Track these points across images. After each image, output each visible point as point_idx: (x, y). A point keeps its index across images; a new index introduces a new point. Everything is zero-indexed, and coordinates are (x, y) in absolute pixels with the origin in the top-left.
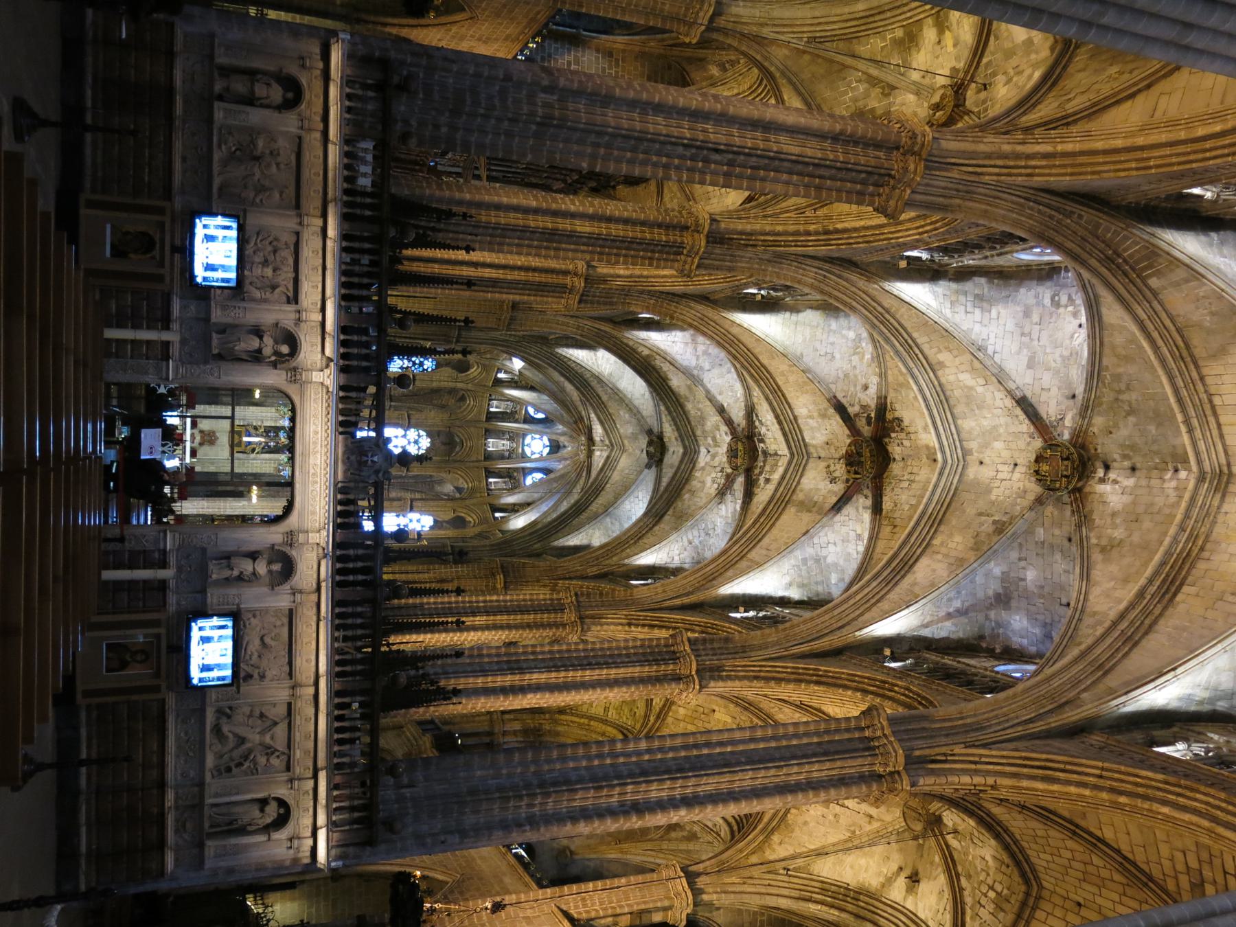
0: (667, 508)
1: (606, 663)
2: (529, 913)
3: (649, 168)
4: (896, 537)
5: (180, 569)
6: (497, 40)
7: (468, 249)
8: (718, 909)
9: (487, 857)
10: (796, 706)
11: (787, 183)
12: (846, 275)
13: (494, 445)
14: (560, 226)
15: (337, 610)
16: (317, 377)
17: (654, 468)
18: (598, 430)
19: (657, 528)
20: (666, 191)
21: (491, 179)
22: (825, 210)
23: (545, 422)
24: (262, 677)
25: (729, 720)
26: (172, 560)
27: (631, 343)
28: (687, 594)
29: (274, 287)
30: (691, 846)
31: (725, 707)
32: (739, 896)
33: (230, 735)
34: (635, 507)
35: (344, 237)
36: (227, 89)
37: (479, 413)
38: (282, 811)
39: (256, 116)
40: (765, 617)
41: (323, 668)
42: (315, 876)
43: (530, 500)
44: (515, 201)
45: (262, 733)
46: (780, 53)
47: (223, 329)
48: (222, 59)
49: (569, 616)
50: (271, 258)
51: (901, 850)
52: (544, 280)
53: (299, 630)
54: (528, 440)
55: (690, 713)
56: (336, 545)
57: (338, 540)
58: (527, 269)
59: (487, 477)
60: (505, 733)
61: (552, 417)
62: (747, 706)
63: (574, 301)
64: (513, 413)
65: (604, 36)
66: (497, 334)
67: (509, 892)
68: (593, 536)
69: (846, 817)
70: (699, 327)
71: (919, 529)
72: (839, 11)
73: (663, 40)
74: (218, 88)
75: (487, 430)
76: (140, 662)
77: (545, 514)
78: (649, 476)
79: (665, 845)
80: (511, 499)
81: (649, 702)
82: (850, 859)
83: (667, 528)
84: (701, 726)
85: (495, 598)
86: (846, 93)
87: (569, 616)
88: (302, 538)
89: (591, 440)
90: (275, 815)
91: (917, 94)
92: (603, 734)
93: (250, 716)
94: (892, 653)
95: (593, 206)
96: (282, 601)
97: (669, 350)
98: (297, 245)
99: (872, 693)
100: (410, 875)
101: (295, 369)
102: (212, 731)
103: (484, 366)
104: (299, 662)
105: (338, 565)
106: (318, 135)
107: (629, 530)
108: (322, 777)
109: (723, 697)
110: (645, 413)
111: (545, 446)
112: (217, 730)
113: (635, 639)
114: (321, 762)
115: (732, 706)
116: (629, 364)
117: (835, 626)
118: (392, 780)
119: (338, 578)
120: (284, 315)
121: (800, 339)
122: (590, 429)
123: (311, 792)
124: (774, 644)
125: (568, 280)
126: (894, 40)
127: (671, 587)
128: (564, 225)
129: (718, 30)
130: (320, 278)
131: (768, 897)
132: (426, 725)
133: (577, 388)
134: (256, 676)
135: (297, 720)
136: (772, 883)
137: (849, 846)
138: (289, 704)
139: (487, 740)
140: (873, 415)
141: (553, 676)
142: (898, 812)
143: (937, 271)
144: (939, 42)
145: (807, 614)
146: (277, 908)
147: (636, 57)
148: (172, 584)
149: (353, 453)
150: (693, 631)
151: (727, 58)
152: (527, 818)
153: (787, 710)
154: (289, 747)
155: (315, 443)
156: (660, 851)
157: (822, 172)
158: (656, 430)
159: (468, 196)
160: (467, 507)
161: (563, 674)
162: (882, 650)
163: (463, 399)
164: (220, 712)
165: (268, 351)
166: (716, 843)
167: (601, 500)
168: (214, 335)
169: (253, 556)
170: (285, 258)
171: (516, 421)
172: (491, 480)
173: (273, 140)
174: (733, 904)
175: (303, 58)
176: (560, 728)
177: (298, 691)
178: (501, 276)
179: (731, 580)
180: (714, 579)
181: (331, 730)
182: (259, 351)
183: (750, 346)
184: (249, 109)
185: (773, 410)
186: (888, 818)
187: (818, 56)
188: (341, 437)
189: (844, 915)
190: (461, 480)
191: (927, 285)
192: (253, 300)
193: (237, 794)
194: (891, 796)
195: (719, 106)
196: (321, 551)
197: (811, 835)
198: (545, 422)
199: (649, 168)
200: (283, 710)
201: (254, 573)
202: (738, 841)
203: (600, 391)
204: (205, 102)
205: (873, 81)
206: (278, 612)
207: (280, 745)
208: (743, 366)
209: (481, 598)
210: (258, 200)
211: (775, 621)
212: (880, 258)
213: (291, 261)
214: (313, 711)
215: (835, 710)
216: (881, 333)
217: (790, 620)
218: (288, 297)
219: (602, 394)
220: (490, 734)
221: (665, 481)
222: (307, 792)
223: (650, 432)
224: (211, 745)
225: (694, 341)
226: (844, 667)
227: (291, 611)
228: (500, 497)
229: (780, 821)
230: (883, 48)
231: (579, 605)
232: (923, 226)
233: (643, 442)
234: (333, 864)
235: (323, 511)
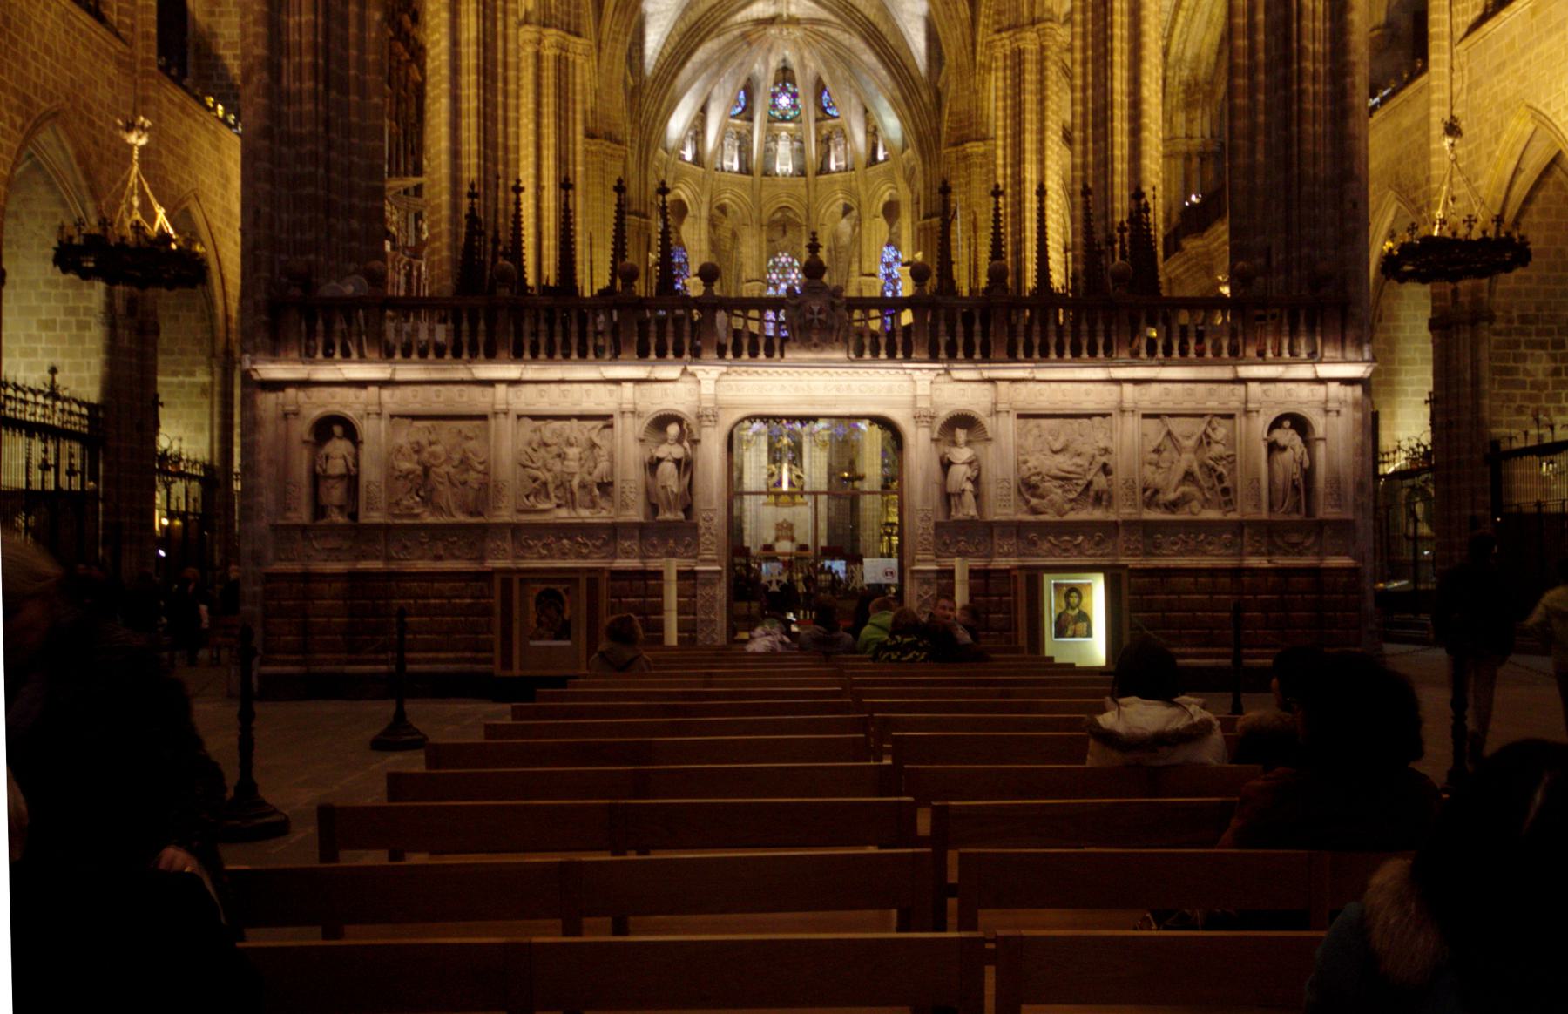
5: (961, 554)
6: (221, 163)
7: (518, 190)
9: (1381, 140)
13: (784, 164)
14: (473, 62)
15: (1021, 356)
16: (708, 388)
21: (418, 171)
23: (749, 89)
24: (1106, 451)
26: (947, 563)
29: (593, 445)
33: (1181, 489)
35: (517, 356)
36: (341, 508)
37: (740, 185)
38: (1287, 424)
39: (371, 472)
41: (1099, 373)
43: (860, 110)
44: (444, 130)
47: (653, 508)
48: (303, 515)
49: (1029, 41)
50: (555, 450)
52: (552, 90)
53: (1045, 405)
56: (934, 358)
57: (926, 357)
58: (538, 114)
59: (829, 172)
60: (1189, 137)
63: (579, 45)
64: (740, 137)
74: (339, 519)
75: (765, 174)
76: (1080, 597)
77: (881, 87)
80: (859, 137)
85: (1000, 152)
87: (1029, 41)
88: (923, 404)
90: (1292, 432)
93: (1157, 466)
95: (438, 11)
96: (1006, 428)
98: (535, 417)
101: (699, 416)
104: (1089, 405)
105: (960, 355)
106: (386, 394)
108: (1245, 371)
112: (1173, 506)
114: (1226, 373)
118: (1260, 279)
119: (977, 356)
120: (628, 433)
123: (1266, 386)
125: (549, 53)
128: (470, 57)
130: (576, 386)
133: (701, 41)
134: (1104, 459)
135: (1167, 405)
138: (1145, 416)
139: (1196, 162)
141: (1120, 58)
148: (978, 563)
149: (809, 339)
154: (1202, 416)
155: (796, 389)
159: (445, 198)
160: (870, 199)
161: (1117, 44)
163: (723, 209)
164: (1150, 503)
165: (678, 452)
168: (660, 517)
169: (946, 465)
170: (554, 432)
171: (751, 132)
172: (833, 167)
173: (399, 449)
175: (286, 415)
176: (1189, 54)
177: (1127, 405)
178: (552, 152)
181: (1184, 361)
182: (678, 462)
184: (363, 481)
188: (788, 355)
190: (834, 208)
192: (611, 472)
193: (1258, 480)
196: (941, 379)
200: (1152, 424)
201: (970, 464)
204: (361, 535)
206: (1021, 434)
207: (1199, 426)
209: (1000, 172)
210: (481, 468)
213: (557, 424)
214: (1155, 386)
218: (605, 427)
220: (1188, 157)
222: (1265, 392)
227: (1020, 416)
228: (856, 153)
231: (1016, 27)
235: (887, 377)
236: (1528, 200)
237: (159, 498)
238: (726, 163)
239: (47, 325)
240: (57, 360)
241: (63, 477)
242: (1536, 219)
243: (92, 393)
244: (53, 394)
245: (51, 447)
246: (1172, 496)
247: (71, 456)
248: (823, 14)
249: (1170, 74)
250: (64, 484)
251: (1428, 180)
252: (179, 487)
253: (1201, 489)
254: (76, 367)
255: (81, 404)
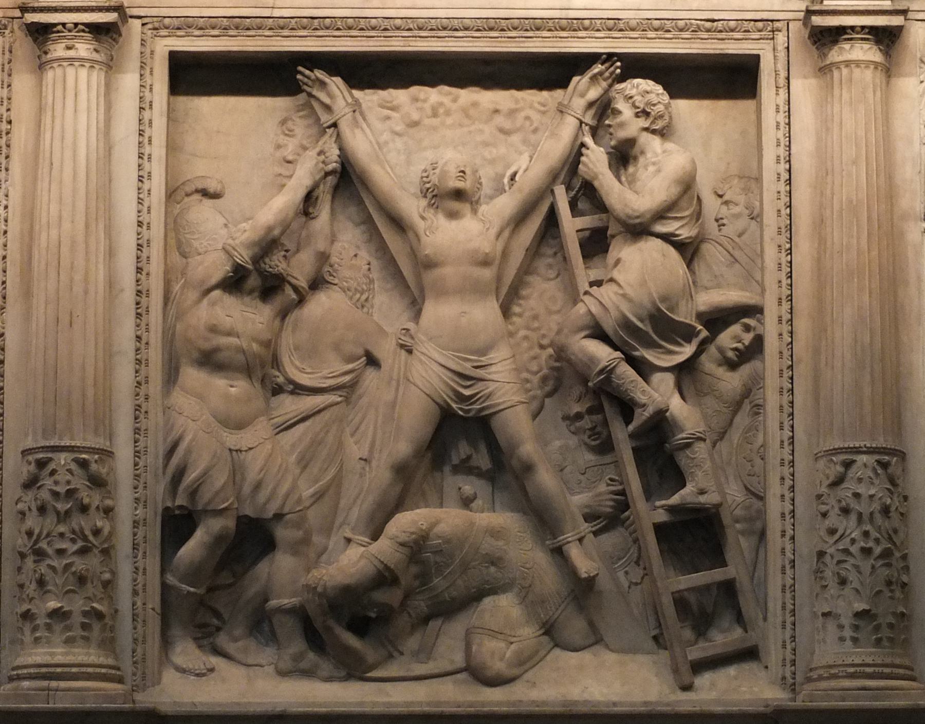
45: (412, 278)
93: (263, 371)
102: (354, 669)
200: (237, 125)
224: (479, 675)
246: (350, 561)
253: (543, 519)
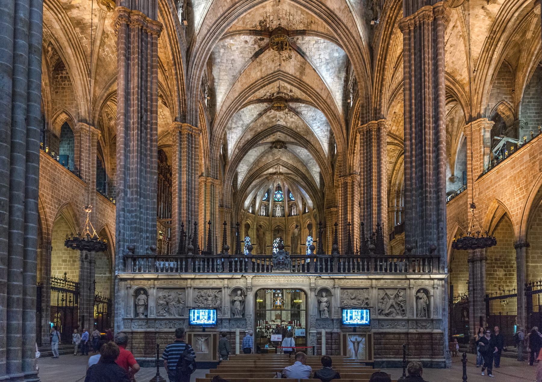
0: (304, 138)
1: (370, 162)
2: (477, 193)
3: (153, 148)
4: (316, 21)
8: (488, 105)
10: (395, 70)
11: (152, 83)
12: (194, 54)
13: (278, 213)
17: (287, 145)
18: (271, 170)
19: (312, 143)
20: (167, 143)
22: (165, 65)
23: (268, 192)
25: (399, 105)
27: (234, 157)
28: (341, 127)
30: (456, 121)
31: (393, 107)
32: (484, 95)
34: (303, 153)
37: (265, 219)
40: (353, 89)
42: (449, 279)
46: (99, 92)
51: (473, 8)
54: (276, 199)
55: (395, 124)
59: (292, 216)
60: (398, 206)
61: (266, 190)
62: (394, 95)
64: (265, 206)
65: (107, 172)
66: (234, 213)
67: (467, 202)
68: (315, 171)
69: (453, 41)
70: (226, 129)
71: (313, 8)
72: (74, 63)
73: (103, 146)
75: (273, 216)
77: (307, 191)
78: (290, 147)
79: (454, 133)
80: (301, 206)
81: (389, 143)
82: (473, 37)
83: (312, 138)
84: (401, 119)
86: (110, 57)
89: (275, 174)
91: (104, 18)
92: (401, 164)
94: (373, 20)
97: (235, 140)
99: (392, 29)
100: (454, 242)
103: (247, 218)
107: (313, 155)
109: (389, 108)
110: (263, 150)
111: (279, 193)
113: (360, 150)
115: (393, 103)
116: (242, 158)
117: (359, 52)
121: (226, 77)
122: (271, 174)
124: (366, 83)
126: (82, 32)
127: (338, 135)
129: (93, 121)
131: (487, 80)
132: (392, 237)
133: (254, 180)
136: (480, 79)
137: (467, 39)
140: (259, 37)
142: (454, 11)
143: (188, 4)
144: (78, 7)
145: (353, 67)
146: (460, 292)
147: (113, 158)
150: (358, 124)
151: (106, 117)
152: (436, 194)
153: (397, 75)
156: (457, 135)
157: (144, 65)
158: (270, 145)
160: (304, 223)
162: (371, 25)
163: (260, 226)
166: (457, 109)
167: (300, 168)
171: (269, 205)
174: (487, 98)
176: (397, 183)
179: (335, 107)
180: (335, 115)
183: (231, 102)
185: (259, 89)
186: (456, 16)
187: (96, 72)
189: (502, 39)
191: (194, 9)
194: (446, 12)
195: (121, 117)
197: (459, 59)
198: (268, 192)
199: (153, 148)
202: (457, 97)
203: (255, 170)
205: (102, 44)
208: (240, 105)
211: (355, 84)
212: (184, 35)
215: (399, 49)
216: (220, 34)
217: (355, 76)
219: (256, 169)
221: (292, 140)
223: (271, 148)
225: (230, 129)
226: (379, 45)
228: (299, 210)
229: (451, 76)
230: (86, 39)
232: (166, 12)
233: (275, 151)
234: (446, 272)
236: (497, 226)
237: (95, 308)
238: (262, 213)
239: (64, 261)
240: (67, 271)
241: (68, 303)
242: (499, 231)
243: (76, 280)
244: (65, 280)
245: (65, 295)
247: (70, 297)
248: (290, 172)
249: (391, 188)
250: (68, 305)
251: (467, 220)
252: (101, 305)
254: (72, 273)
255: (73, 283)
